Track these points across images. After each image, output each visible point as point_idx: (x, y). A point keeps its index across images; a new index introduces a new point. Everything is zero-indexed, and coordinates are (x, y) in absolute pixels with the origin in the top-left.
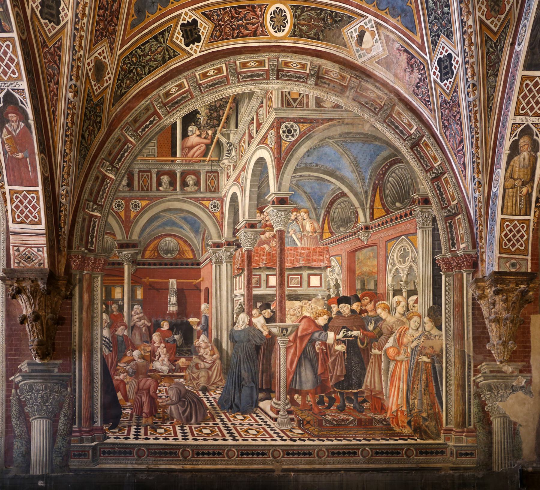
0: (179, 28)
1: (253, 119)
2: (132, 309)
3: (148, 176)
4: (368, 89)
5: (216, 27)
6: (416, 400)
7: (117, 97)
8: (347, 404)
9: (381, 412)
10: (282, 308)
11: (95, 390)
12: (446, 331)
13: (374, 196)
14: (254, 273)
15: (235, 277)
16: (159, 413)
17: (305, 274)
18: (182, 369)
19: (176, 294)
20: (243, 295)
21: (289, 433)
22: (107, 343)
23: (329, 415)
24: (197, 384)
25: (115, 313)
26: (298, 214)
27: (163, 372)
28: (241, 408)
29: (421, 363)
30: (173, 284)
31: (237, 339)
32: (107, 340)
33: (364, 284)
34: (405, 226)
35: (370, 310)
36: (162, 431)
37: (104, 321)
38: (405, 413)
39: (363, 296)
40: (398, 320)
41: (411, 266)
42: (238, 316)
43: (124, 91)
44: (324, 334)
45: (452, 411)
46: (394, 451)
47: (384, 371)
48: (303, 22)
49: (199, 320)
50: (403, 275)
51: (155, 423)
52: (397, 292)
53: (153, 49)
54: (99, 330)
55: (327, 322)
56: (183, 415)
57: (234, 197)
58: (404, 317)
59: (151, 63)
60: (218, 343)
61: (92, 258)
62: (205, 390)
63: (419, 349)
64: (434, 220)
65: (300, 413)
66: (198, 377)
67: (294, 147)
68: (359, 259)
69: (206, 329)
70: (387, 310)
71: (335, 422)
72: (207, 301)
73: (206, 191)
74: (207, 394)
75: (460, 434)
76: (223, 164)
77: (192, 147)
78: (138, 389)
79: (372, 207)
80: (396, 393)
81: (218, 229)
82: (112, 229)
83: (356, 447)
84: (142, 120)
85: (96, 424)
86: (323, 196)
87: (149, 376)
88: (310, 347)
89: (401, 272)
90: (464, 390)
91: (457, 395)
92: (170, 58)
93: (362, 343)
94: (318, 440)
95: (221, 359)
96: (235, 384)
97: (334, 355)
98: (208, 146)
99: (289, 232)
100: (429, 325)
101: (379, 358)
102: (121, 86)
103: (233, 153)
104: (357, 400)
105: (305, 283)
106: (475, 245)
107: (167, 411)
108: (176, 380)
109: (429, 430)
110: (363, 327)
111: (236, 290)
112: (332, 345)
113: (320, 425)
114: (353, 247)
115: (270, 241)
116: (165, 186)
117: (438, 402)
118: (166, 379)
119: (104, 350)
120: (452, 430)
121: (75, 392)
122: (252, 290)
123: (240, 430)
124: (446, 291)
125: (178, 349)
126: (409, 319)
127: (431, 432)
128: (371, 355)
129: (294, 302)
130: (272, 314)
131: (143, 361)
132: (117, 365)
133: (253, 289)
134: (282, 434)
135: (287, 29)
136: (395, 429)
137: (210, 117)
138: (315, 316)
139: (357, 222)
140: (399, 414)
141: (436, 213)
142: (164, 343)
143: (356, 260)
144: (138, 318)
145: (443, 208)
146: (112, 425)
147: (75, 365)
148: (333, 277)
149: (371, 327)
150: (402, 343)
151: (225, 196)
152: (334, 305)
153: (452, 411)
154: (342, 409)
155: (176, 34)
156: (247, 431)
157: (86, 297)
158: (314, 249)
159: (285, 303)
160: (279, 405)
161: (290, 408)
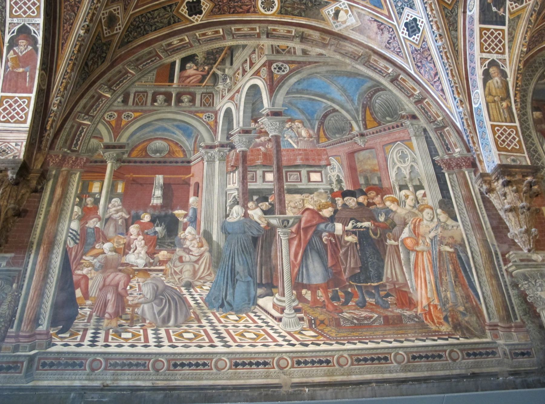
0: (185, 4)
1: (246, 60)
2: (110, 202)
3: (144, 95)
4: (346, 46)
5: (216, 5)
6: (448, 293)
7: (123, 43)
8: (367, 299)
9: (410, 307)
10: (282, 201)
11: (48, 286)
12: (462, 222)
13: (365, 112)
14: (249, 169)
15: (228, 173)
16: (127, 314)
17: (304, 171)
18: (162, 263)
19: (162, 188)
20: (237, 189)
21: (298, 336)
22: (74, 235)
23: (347, 313)
24: (179, 279)
25: (89, 206)
26: (293, 124)
27: (137, 266)
28: (234, 306)
29: (444, 253)
30: (160, 179)
31: (230, 231)
32: (74, 233)
33: (367, 179)
34: (398, 134)
35: (378, 202)
36: (129, 335)
37: (74, 213)
38: (439, 307)
39: (369, 190)
40: (410, 212)
41: (412, 166)
42: (231, 207)
43: (130, 39)
44: (330, 225)
45: (492, 303)
46: (434, 355)
47: (405, 262)
48: (288, 5)
49: (186, 212)
50: (406, 172)
51: (120, 325)
52: (401, 188)
53: (161, 15)
54: (67, 222)
55: (332, 213)
56: (159, 316)
57: (228, 112)
58: (415, 209)
59: (158, 24)
60: (208, 236)
61: (74, 157)
62: (189, 286)
63: (438, 239)
64: (425, 130)
65: (310, 311)
66: (181, 271)
67: (284, 79)
68: (358, 159)
69: (194, 221)
70: (396, 203)
71: (355, 321)
72: (196, 194)
73: (201, 106)
74: (192, 290)
75: (508, 330)
76: (219, 88)
77: (189, 77)
78: (104, 286)
79: (364, 120)
80: (423, 285)
81: (211, 134)
82: (101, 134)
83: (386, 351)
84: (144, 59)
85: (41, 327)
86: (316, 111)
87: (120, 271)
88: (316, 239)
89: (403, 169)
90: (498, 280)
91: (492, 285)
92: (175, 22)
93: (376, 234)
94: (337, 343)
95: (210, 251)
96: (227, 279)
97: (344, 246)
98: (204, 78)
99: (285, 137)
100: (443, 217)
101: (397, 249)
102: (129, 35)
103: (228, 81)
104: (379, 294)
105: (304, 179)
106: (469, 150)
107: (139, 311)
108: (154, 274)
109: (471, 326)
110: (373, 218)
111: (229, 184)
112: (342, 236)
113: (338, 325)
114: (351, 150)
115: (266, 144)
116: (160, 103)
117: (473, 293)
118: (141, 274)
119: (68, 242)
120: (498, 326)
121: (22, 289)
122: (247, 184)
123: (233, 334)
124: (452, 186)
125: (159, 241)
126: (422, 211)
127: (474, 328)
128: (387, 246)
129: (295, 195)
130: (270, 206)
131: (114, 253)
132: (81, 258)
133: (249, 184)
134: (289, 337)
135: (275, 9)
136: (430, 327)
137: (207, 58)
138: (318, 208)
139: (351, 130)
140: (432, 308)
141: (425, 126)
142: (143, 235)
143: (356, 159)
144: (115, 211)
145: (431, 122)
146: (62, 329)
147: (29, 258)
148: (333, 174)
149: (382, 219)
150: (418, 234)
151: (219, 110)
152: (339, 198)
153: (492, 303)
154: (363, 305)
155: (182, 8)
156: (242, 335)
157: (59, 191)
158: (312, 151)
159: (284, 196)
160: (284, 301)
161: (298, 305)
